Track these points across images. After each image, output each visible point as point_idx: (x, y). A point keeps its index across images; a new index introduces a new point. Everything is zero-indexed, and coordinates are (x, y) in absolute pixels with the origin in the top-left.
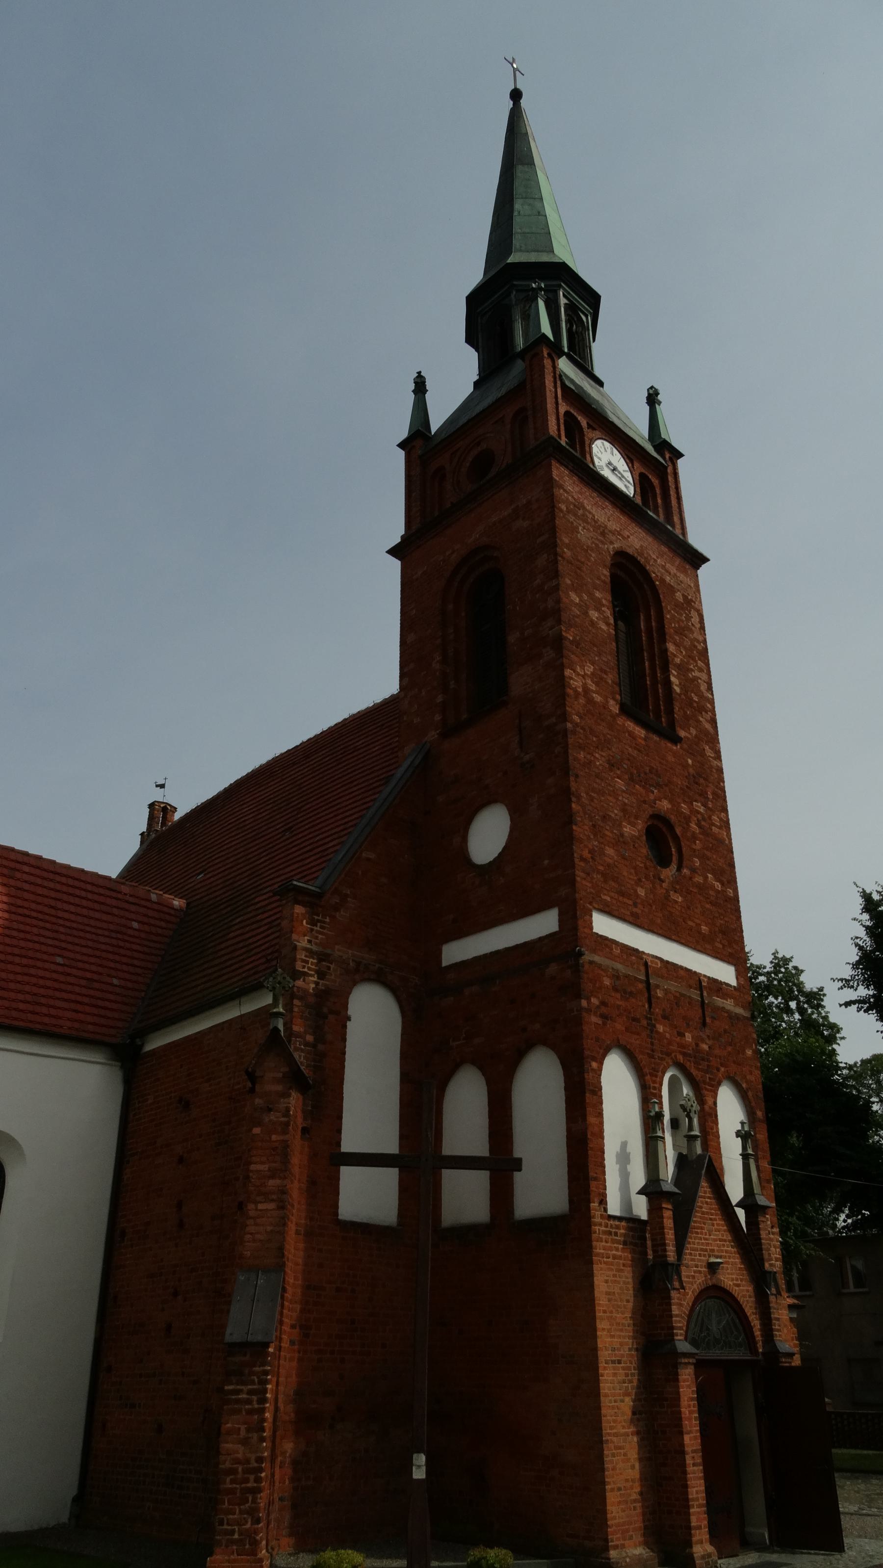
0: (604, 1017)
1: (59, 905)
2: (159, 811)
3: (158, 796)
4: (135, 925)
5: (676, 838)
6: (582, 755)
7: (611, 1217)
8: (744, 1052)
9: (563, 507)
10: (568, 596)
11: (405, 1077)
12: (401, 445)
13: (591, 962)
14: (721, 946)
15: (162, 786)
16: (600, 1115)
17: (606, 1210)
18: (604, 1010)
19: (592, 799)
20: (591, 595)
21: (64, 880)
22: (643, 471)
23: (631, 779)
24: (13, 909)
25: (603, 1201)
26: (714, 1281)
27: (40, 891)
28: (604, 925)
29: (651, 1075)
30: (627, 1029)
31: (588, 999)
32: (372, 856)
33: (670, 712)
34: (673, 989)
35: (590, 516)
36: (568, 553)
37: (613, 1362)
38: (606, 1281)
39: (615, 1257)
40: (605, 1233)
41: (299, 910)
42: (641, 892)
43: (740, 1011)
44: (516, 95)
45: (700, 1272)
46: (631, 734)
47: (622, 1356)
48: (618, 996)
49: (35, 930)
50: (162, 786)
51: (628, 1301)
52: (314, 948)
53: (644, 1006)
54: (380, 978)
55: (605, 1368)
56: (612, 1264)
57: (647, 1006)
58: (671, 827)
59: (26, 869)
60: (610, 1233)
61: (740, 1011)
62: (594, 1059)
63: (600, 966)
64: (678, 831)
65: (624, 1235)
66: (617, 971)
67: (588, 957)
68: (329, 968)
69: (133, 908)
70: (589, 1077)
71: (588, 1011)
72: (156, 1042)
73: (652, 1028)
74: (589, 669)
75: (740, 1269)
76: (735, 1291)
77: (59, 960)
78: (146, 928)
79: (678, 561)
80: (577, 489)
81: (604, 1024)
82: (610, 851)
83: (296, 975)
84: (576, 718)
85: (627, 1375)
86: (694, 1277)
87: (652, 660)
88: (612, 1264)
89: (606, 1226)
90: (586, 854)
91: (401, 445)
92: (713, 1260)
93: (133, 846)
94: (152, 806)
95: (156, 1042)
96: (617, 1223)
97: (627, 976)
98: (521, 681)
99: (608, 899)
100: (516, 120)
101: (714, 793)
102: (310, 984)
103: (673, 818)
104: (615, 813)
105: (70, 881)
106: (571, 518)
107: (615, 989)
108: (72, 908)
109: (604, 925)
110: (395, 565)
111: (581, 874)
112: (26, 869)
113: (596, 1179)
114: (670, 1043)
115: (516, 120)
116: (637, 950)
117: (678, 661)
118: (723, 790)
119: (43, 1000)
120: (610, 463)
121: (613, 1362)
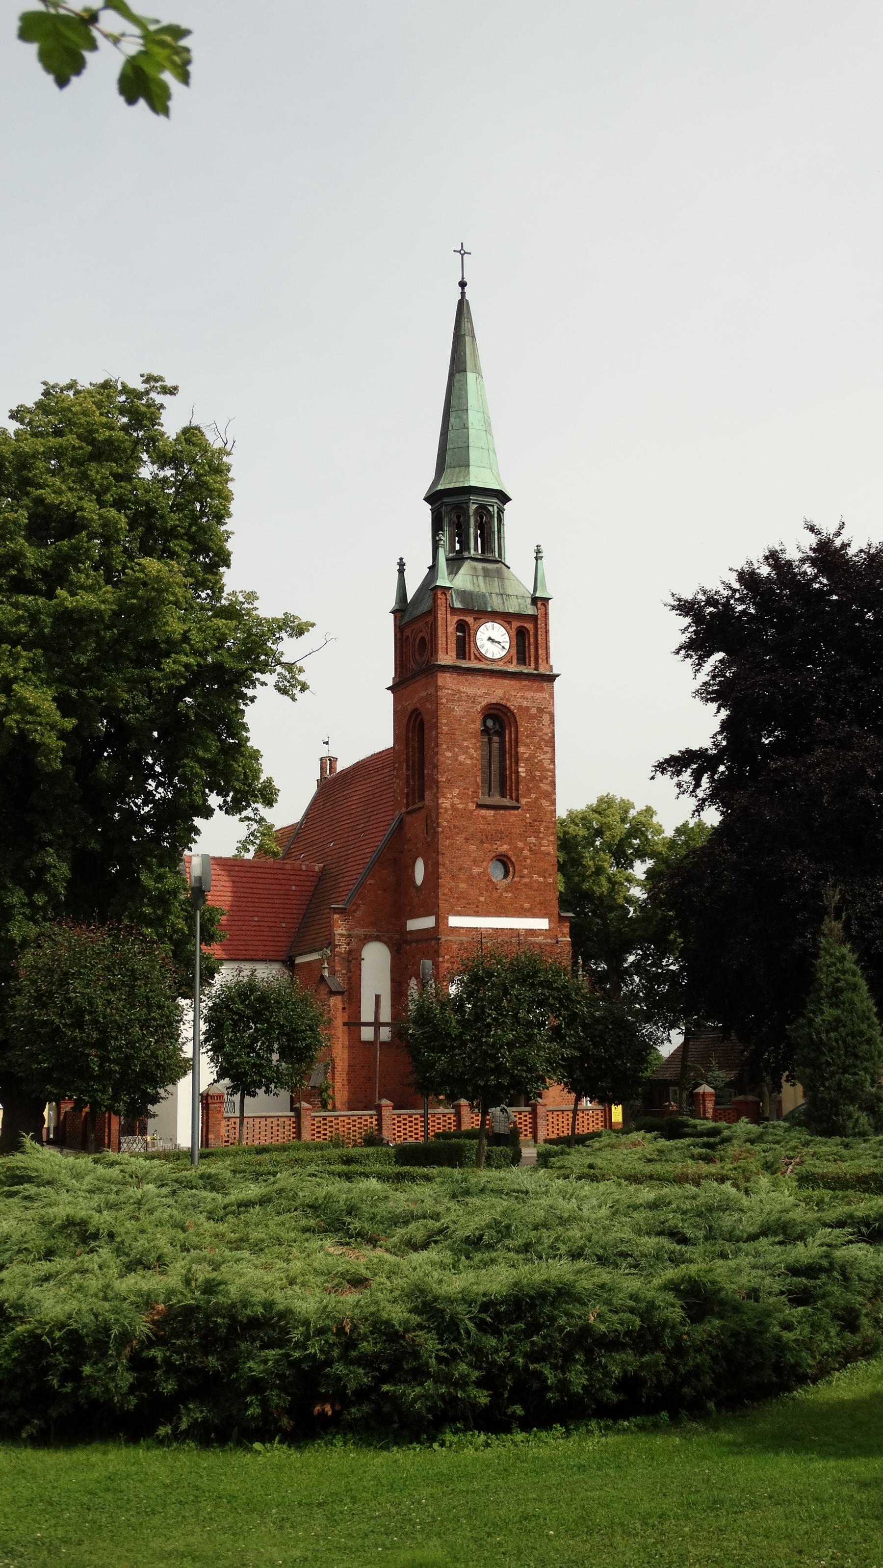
1: (254, 885)
2: (327, 763)
3: (325, 752)
4: (294, 888)
9: (444, 701)
10: (444, 755)
11: (393, 981)
12: (392, 612)
15: (327, 743)
20: (461, 747)
21: (255, 870)
22: (519, 624)
23: (482, 842)
24: (237, 879)
27: (244, 880)
28: (454, 921)
32: (372, 882)
33: (517, 790)
41: (336, 916)
42: (482, 899)
44: (463, 284)
46: (484, 817)
50: (327, 743)
52: (344, 932)
54: (378, 939)
58: (509, 858)
59: (237, 869)
64: (513, 859)
67: (443, 939)
69: (292, 877)
72: (299, 960)
74: (456, 792)
77: (256, 919)
78: (300, 888)
82: (463, 885)
83: (336, 946)
84: (445, 824)
87: (511, 759)
90: (447, 891)
91: (392, 612)
93: (313, 789)
94: (321, 759)
95: (299, 960)
98: (428, 795)
100: (463, 307)
102: (343, 949)
103: (510, 853)
104: (468, 864)
105: (259, 870)
106: (450, 705)
108: (260, 886)
109: (454, 921)
110: (390, 695)
112: (237, 869)
115: (463, 307)
117: (526, 756)
120: (490, 639)
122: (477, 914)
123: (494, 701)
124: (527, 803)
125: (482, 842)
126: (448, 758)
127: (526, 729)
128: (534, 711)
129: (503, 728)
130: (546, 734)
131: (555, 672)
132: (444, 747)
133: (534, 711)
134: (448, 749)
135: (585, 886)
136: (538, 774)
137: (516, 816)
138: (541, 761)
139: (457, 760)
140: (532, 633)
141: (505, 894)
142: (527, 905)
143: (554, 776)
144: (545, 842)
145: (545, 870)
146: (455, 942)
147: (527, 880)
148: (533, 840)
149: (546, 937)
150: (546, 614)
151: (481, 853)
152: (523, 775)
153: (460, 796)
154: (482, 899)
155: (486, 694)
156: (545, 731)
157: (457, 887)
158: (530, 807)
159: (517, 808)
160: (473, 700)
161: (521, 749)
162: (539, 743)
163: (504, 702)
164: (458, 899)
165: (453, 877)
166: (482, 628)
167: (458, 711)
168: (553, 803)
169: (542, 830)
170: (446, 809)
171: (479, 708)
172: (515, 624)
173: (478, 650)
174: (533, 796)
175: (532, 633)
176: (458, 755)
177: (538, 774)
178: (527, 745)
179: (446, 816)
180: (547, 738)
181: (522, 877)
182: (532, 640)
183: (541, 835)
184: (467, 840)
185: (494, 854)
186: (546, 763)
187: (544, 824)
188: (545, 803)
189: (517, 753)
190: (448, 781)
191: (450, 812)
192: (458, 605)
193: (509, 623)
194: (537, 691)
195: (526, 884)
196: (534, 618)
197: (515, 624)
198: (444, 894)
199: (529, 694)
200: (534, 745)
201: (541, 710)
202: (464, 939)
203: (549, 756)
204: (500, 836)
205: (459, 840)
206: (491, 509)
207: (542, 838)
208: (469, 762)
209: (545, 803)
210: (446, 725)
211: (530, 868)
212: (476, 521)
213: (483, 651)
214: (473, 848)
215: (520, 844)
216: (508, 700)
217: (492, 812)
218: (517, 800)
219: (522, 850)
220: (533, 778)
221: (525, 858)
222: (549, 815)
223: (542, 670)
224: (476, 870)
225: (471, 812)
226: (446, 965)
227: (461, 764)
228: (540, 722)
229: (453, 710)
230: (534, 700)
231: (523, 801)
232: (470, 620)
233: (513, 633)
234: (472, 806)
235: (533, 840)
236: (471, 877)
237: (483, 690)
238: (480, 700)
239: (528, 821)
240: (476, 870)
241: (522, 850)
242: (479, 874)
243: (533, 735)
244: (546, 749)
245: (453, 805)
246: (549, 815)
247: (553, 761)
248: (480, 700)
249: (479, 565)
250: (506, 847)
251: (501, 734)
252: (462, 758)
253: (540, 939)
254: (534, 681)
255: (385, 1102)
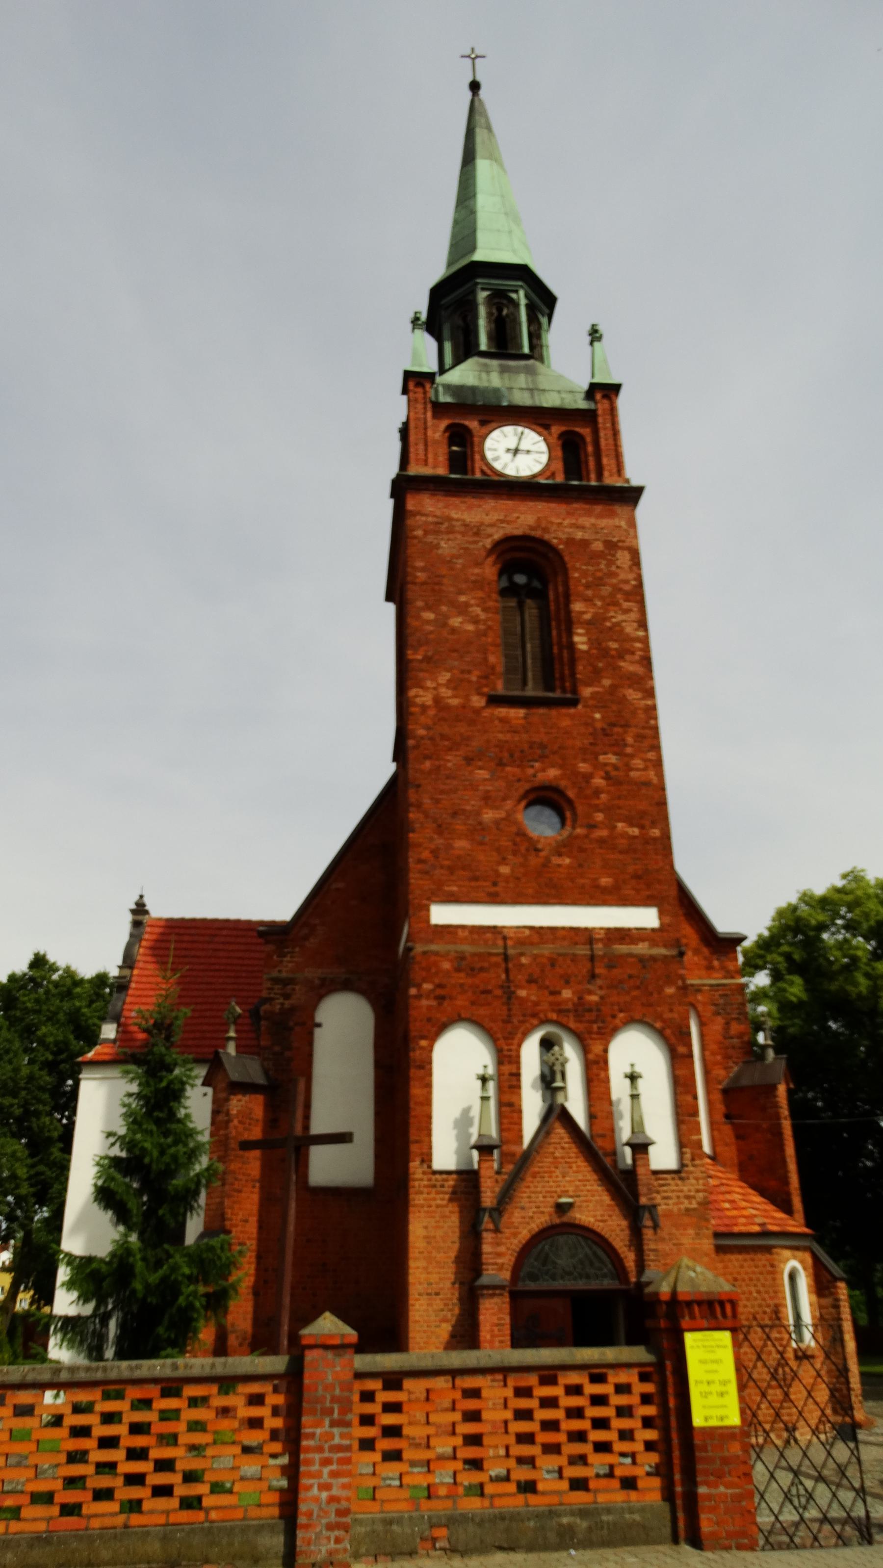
0: (441, 998)
5: (570, 802)
6: (428, 764)
7: (435, 1173)
8: (660, 990)
9: (419, 533)
10: (418, 617)
13: (424, 953)
14: (633, 892)
16: (429, 1086)
17: (430, 1167)
18: (439, 992)
19: (438, 801)
20: (453, 604)
22: (564, 429)
25: (427, 1158)
26: (565, 1219)
29: (505, 1038)
30: (473, 1003)
31: (419, 986)
32: (341, 885)
33: (573, 674)
34: (546, 952)
35: (459, 523)
36: (421, 576)
37: (428, 1294)
38: (426, 1228)
39: (438, 1206)
40: (425, 1186)
42: (505, 870)
43: (663, 951)
45: (542, 1213)
46: (503, 720)
47: (442, 1289)
48: (462, 975)
49: (221, 980)
51: (453, 1242)
53: (499, 977)
54: (346, 986)
55: (417, 1300)
56: (435, 1212)
57: (503, 976)
59: (225, 932)
60: (434, 1186)
61: (663, 951)
62: (423, 1037)
63: (436, 954)
64: (571, 794)
65: (454, 1187)
66: (463, 952)
68: (294, 989)
70: (416, 1055)
71: (418, 997)
73: (510, 995)
74: (444, 677)
75: (608, 1205)
76: (599, 1227)
79: (598, 508)
80: (441, 505)
81: (440, 1004)
82: (461, 844)
85: (446, 1305)
86: (532, 1218)
88: (435, 1212)
89: (430, 1180)
92: (564, 1200)
96: (444, 1176)
97: (474, 955)
99: (455, 889)
100: (473, 110)
101: (640, 737)
103: (563, 784)
106: (430, 538)
107: (458, 970)
111: (418, 875)
112: (225, 932)
113: (417, 1142)
114: (536, 1004)
116: (495, 927)
117: (587, 617)
118: (656, 729)
119: (208, 1035)
121: (428, 1294)
122: (494, 899)
123: (518, 532)
124: (594, 696)
125: (501, 764)
126: (428, 622)
127: (585, 574)
128: (598, 546)
129: (545, 583)
130: (627, 582)
131: (635, 482)
132: (420, 604)
133: (598, 546)
134: (428, 608)
135: (834, 987)
136: (614, 645)
137: (572, 717)
138: (618, 624)
139: (445, 625)
140: (589, 439)
141: (556, 860)
142: (605, 881)
143: (647, 649)
144: (637, 762)
145: (643, 814)
146: (445, 956)
147: (604, 833)
148: (612, 759)
149: (654, 943)
150: (613, 412)
151: (501, 784)
152: (584, 647)
153: (454, 684)
154: (505, 870)
155: (502, 521)
156: (622, 576)
157: (449, 847)
158: (600, 701)
159: (574, 703)
160: (477, 531)
161: (577, 606)
162: (612, 595)
163: (537, 534)
164: (451, 870)
165: (440, 829)
166: (496, 434)
167: (446, 547)
168: (650, 693)
169: (630, 740)
170: (424, 708)
171: (488, 543)
172: (556, 430)
173: (488, 465)
174: (607, 682)
175: (589, 439)
176: (447, 617)
177: (614, 645)
178: (588, 600)
179: (422, 719)
180: (627, 587)
181: (592, 827)
182: (590, 449)
183: (629, 750)
184: (469, 760)
185: (527, 786)
186: (630, 629)
187: (633, 731)
188: (632, 695)
189: (568, 612)
190: (427, 659)
191: (432, 712)
192: (445, 398)
193: (547, 427)
194: (600, 516)
195: (601, 841)
196: (588, 417)
197: (556, 430)
198: (420, 861)
199: (587, 521)
200: (602, 598)
201: (612, 546)
202: (467, 948)
203: (634, 616)
204: (542, 753)
205: (452, 760)
206: (514, 296)
207: (632, 756)
208: (470, 627)
209: (632, 695)
210: (423, 570)
211: (607, 809)
212: (489, 314)
213: (498, 466)
214: (483, 774)
215: (583, 767)
216: (546, 530)
217: (522, 712)
218: (575, 691)
219: (588, 777)
220: (605, 653)
221: (597, 792)
222: (641, 715)
223: (609, 480)
224: (489, 815)
225: (477, 711)
226: (424, 1002)
227: (454, 631)
228: (610, 563)
229: (437, 546)
230: (595, 529)
231: (587, 692)
232: (473, 424)
233: (553, 440)
234: (478, 701)
235: (612, 759)
236: (481, 828)
237: (495, 517)
238: (490, 530)
239: (599, 725)
240: (489, 815)
241: (588, 777)
242: (497, 823)
243: (598, 583)
244: (626, 605)
245: (437, 700)
246: (641, 715)
247: (643, 624)
248: (490, 530)
249: (494, 363)
250: (553, 773)
251: (540, 595)
252: (456, 621)
253: (642, 948)
254: (596, 502)
255: (328, 1325)
